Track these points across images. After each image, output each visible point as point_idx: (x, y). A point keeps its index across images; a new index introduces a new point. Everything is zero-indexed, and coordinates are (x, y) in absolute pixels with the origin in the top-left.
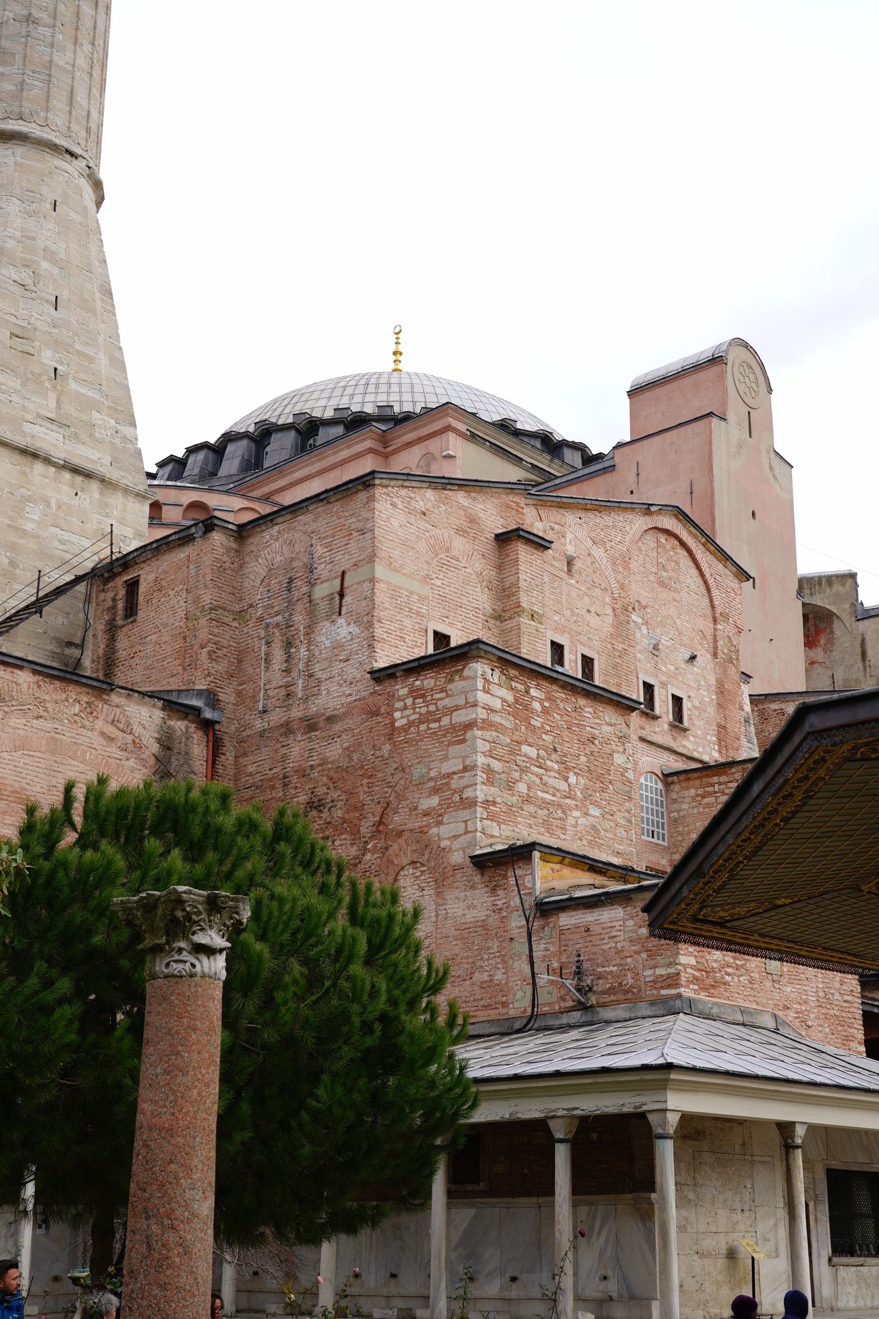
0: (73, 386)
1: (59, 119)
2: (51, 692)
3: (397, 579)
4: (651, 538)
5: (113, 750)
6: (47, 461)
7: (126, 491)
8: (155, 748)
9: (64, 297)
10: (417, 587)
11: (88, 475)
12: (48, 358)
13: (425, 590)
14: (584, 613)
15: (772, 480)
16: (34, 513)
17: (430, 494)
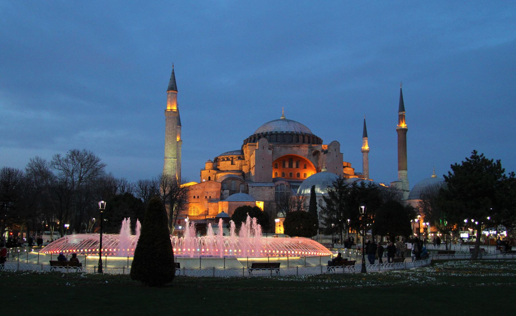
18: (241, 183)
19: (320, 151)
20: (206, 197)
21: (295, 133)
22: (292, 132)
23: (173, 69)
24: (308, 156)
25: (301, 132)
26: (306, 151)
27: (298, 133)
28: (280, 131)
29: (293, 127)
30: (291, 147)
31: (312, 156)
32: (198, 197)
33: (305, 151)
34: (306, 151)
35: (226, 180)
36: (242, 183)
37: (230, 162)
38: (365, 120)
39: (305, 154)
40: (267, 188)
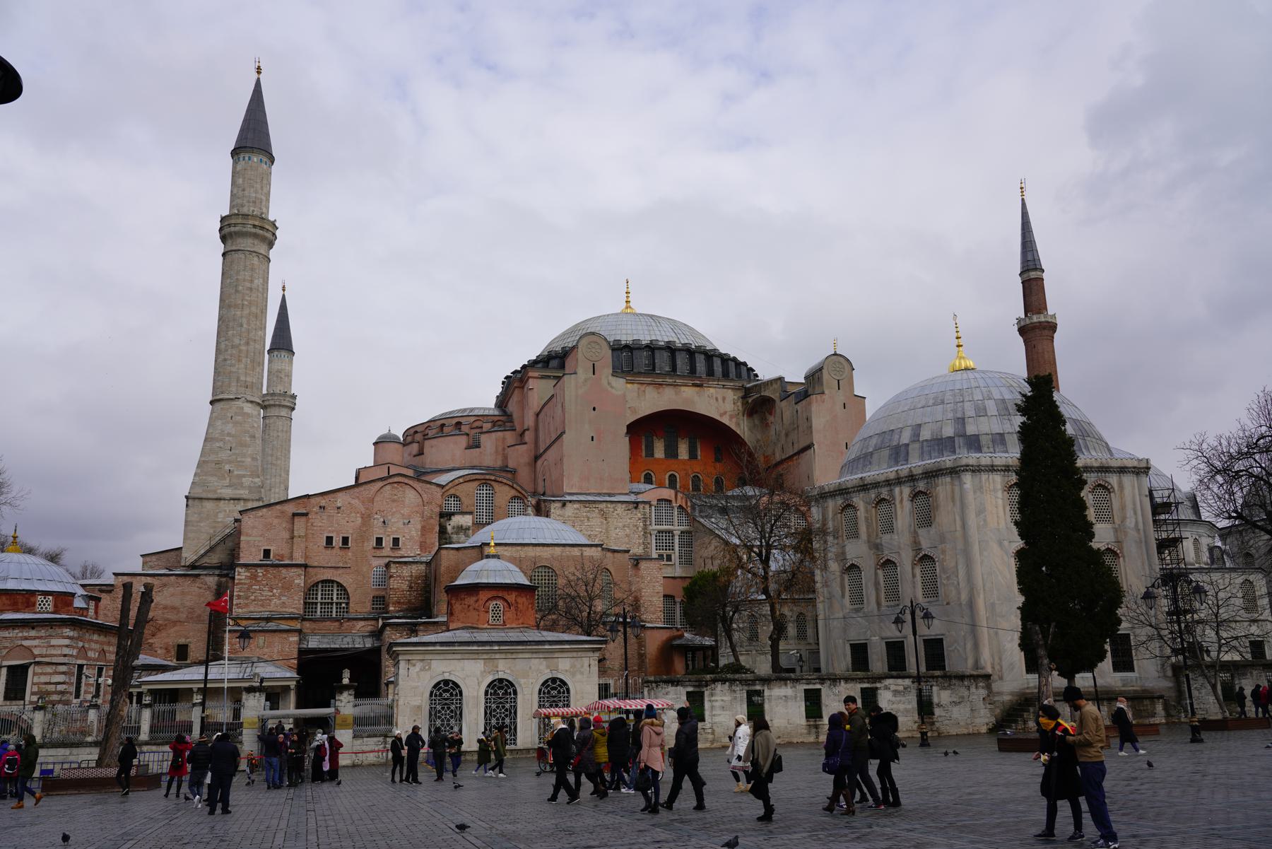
0: (236, 473)
1: (234, 389)
2: (180, 580)
3: (249, 538)
4: (388, 487)
5: (202, 590)
6: (224, 499)
7: (253, 500)
8: (215, 587)
9: (234, 446)
10: (258, 538)
11: (239, 499)
12: (227, 467)
13: (261, 539)
14: (345, 523)
15: (610, 389)
16: (221, 515)
17: (265, 510)
19: (775, 396)
20: (379, 541)
24: (731, 417)
26: (724, 399)
29: (670, 330)
32: (345, 540)
34: (724, 399)
35: (457, 482)
37: (463, 441)
39: (722, 412)
40: (620, 509)
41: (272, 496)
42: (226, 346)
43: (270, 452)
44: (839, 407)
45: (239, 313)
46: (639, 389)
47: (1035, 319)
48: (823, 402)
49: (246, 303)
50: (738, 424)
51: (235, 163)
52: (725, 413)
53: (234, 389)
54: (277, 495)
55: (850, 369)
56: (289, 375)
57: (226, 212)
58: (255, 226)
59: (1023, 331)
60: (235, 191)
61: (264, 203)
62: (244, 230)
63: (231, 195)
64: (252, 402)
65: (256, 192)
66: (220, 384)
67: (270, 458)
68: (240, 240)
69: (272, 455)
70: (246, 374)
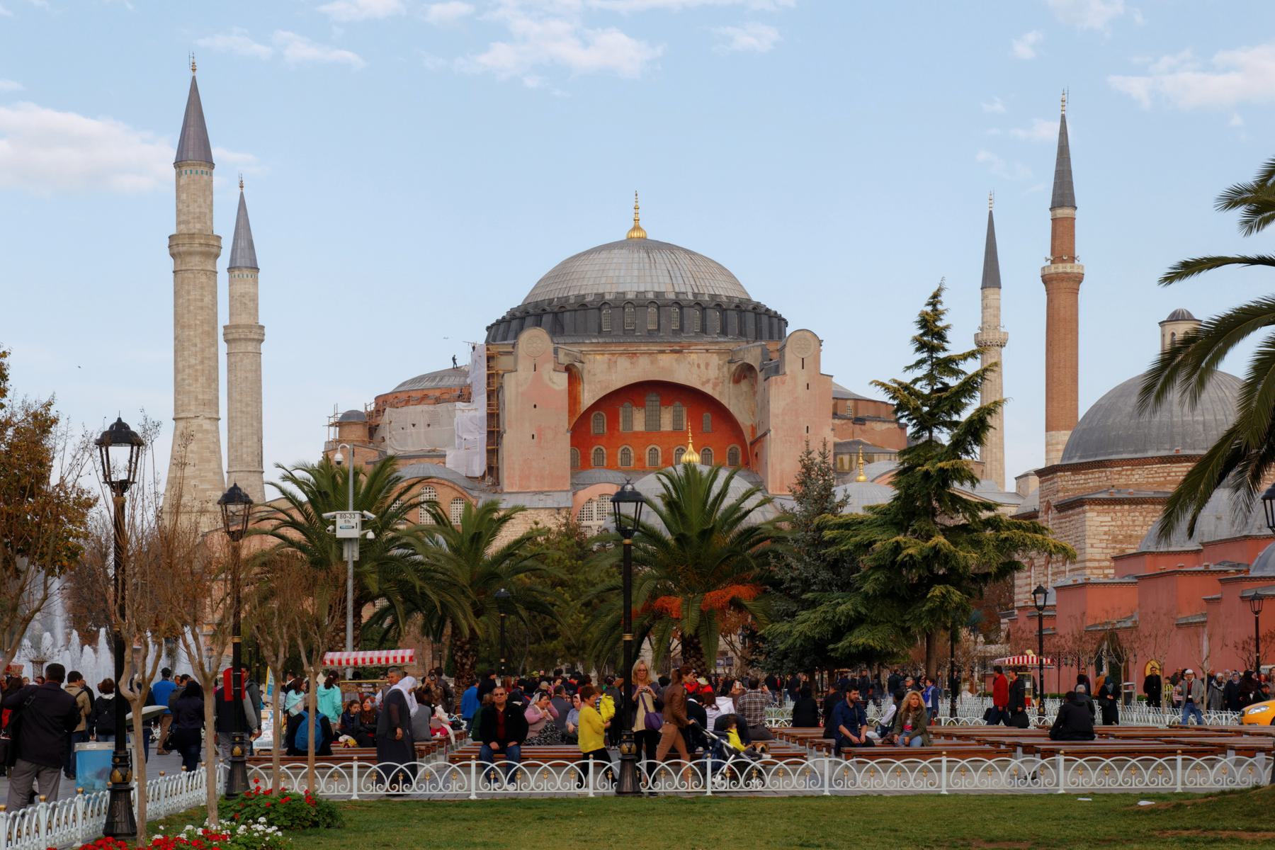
1: (193, 408)
9: (197, 462)
12: (193, 482)
18: (456, 499)
19: (757, 366)
21: (672, 296)
22: (658, 294)
23: (194, 79)
24: (715, 385)
25: (695, 295)
26: (707, 365)
27: (681, 297)
28: (614, 291)
29: (666, 273)
30: (650, 354)
31: (731, 385)
33: (703, 366)
34: (707, 365)
36: (459, 495)
38: (991, 213)
41: (245, 450)
42: (183, 366)
43: (238, 397)
44: (801, 388)
45: (192, 333)
46: (610, 360)
47: (1061, 268)
48: (784, 383)
49: (198, 322)
50: (721, 393)
51: (179, 175)
52: (708, 381)
53: (193, 408)
54: (250, 450)
55: (817, 343)
56: (255, 299)
57: (173, 231)
58: (201, 244)
59: (1047, 280)
60: (180, 207)
61: (208, 216)
62: (192, 249)
63: (177, 210)
64: (210, 418)
65: (200, 207)
66: (180, 402)
67: (238, 405)
68: (188, 259)
69: (241, 401)
70: (204, 392)
